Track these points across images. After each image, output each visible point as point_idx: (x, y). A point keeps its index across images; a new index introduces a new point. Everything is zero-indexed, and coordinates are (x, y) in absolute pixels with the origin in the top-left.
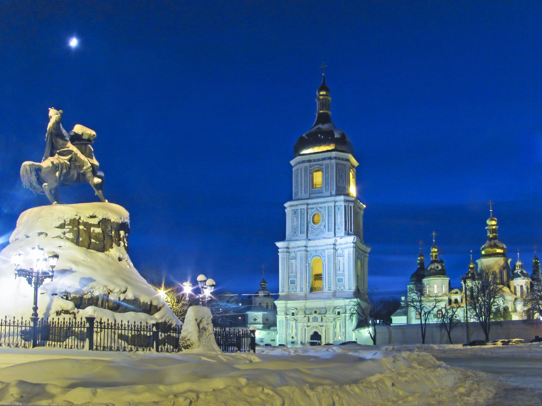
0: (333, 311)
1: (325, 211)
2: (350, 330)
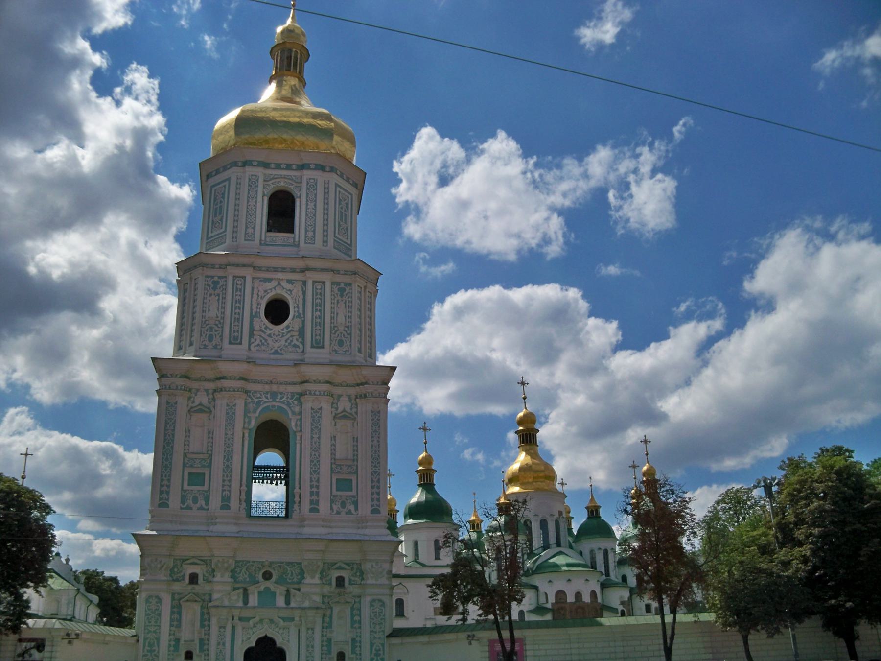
0: (321, 573)
1: (304, 293)
2: (377, 635)
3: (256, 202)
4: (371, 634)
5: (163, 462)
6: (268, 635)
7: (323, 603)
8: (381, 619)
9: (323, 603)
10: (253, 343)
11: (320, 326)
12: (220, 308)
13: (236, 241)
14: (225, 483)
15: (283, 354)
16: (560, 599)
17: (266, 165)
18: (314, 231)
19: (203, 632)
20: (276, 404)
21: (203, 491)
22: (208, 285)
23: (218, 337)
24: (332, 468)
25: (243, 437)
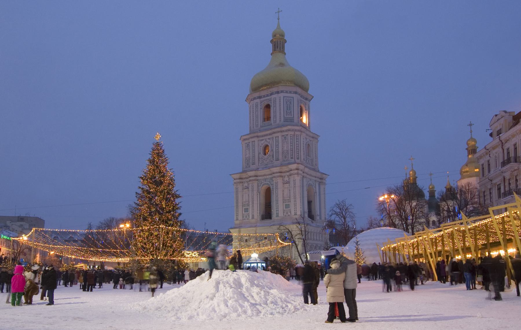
1: (273, 141)
2: (296, 255)
17: (260, 97)
18: (276, 118)
24: (283, 201)
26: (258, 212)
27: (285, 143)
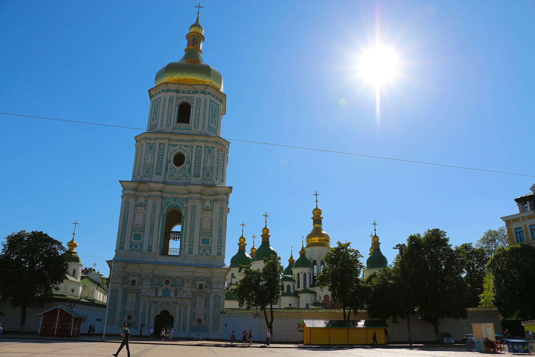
1: (192, 152)
3: (172, 109)
4: (213, 312)
5: (122, 229)
6: (166, 310)
7: (192, 296)
8: (219, 305)
9: (192, 296)
10: (167, 174)
11: (198, 167)
12: (153, 158)
13: (162, 127)
14: (150, 239)
15: (180, 180)
16: (326, 299)
17: (177, 91)
18: (198, 123)
19: (137, 307)
20: (176, 203)
21: (140, 242)
22: (147, 147)
23: (151, 172)
25: (160, 218)
26: (159, 241)
27: (209, 157)
